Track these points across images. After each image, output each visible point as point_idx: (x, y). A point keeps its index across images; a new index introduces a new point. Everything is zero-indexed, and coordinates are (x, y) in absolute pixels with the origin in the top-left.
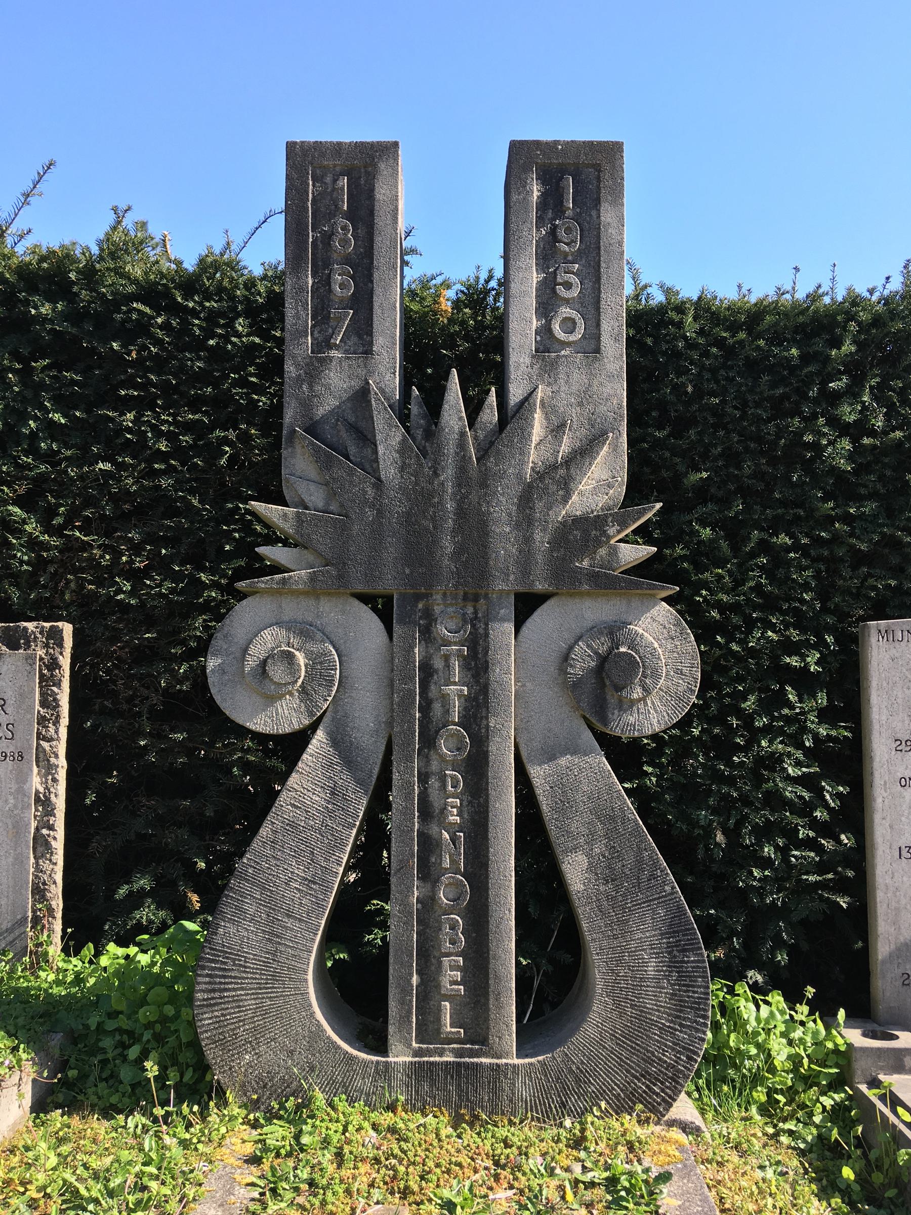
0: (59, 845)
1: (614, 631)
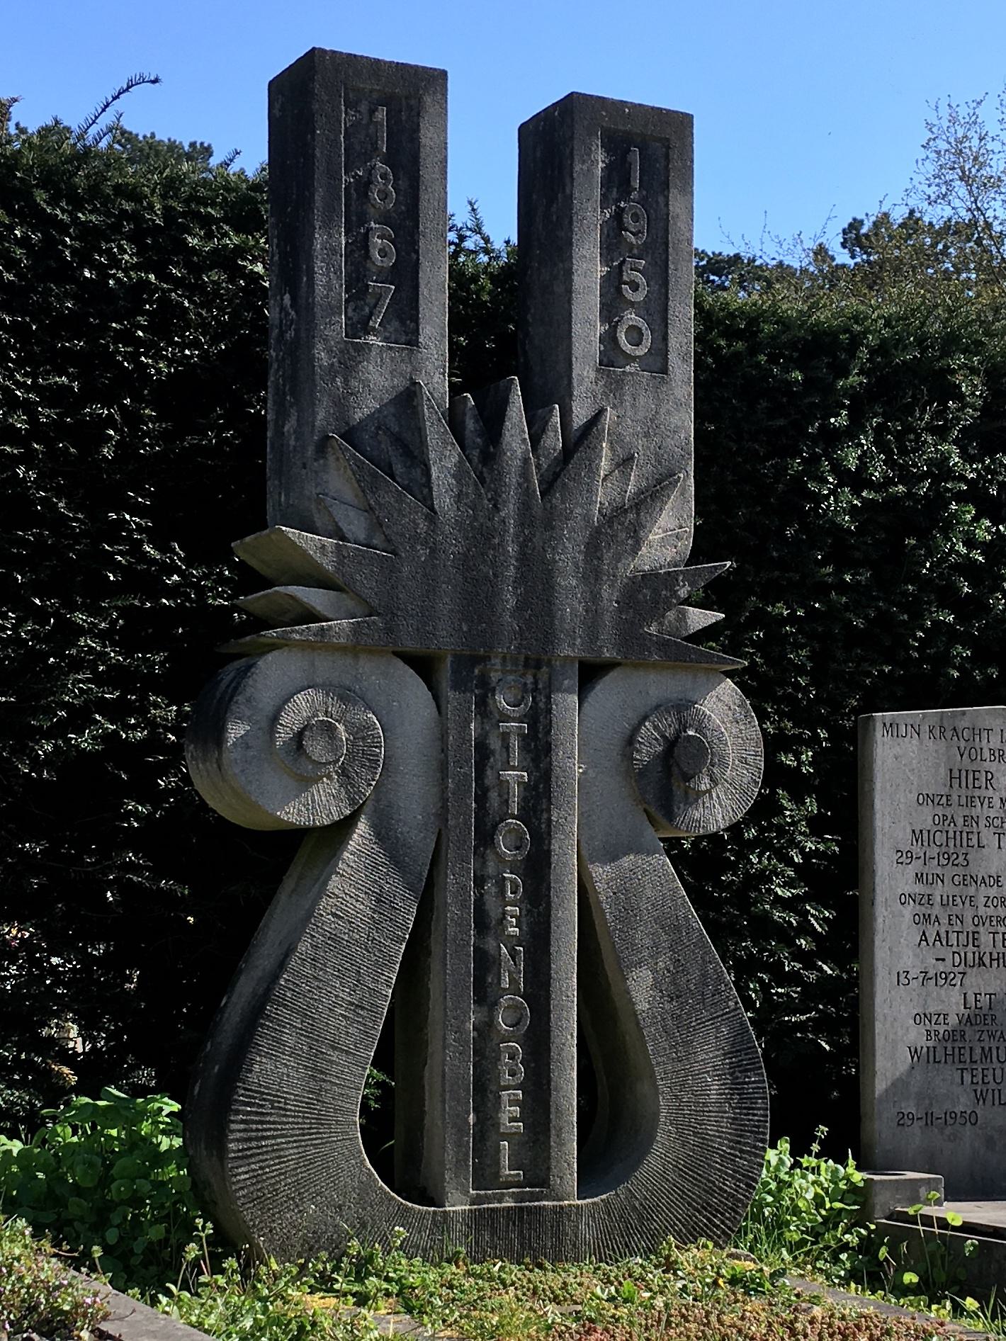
1: (682, 707)
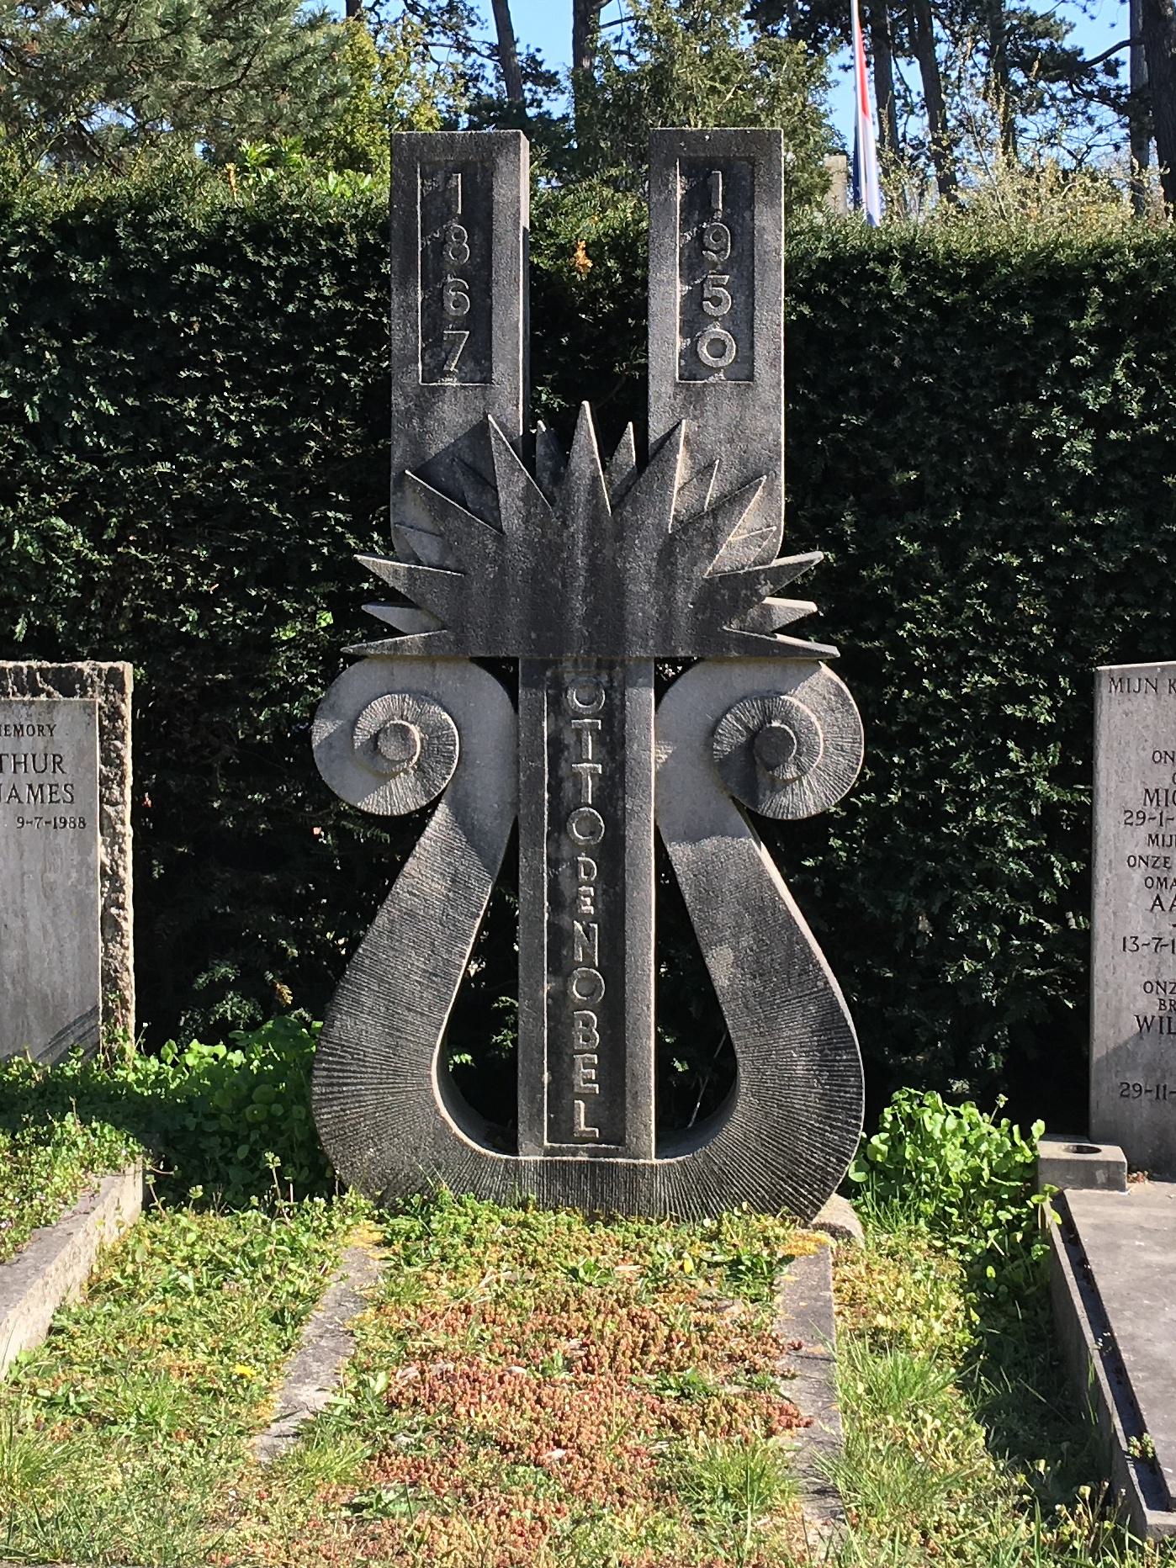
0: (128, 927)
